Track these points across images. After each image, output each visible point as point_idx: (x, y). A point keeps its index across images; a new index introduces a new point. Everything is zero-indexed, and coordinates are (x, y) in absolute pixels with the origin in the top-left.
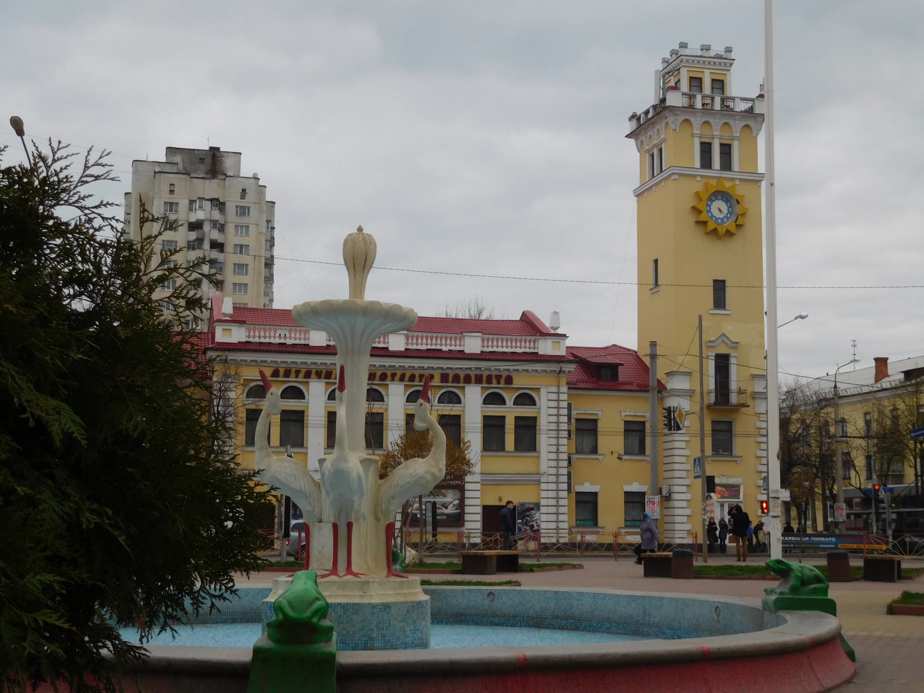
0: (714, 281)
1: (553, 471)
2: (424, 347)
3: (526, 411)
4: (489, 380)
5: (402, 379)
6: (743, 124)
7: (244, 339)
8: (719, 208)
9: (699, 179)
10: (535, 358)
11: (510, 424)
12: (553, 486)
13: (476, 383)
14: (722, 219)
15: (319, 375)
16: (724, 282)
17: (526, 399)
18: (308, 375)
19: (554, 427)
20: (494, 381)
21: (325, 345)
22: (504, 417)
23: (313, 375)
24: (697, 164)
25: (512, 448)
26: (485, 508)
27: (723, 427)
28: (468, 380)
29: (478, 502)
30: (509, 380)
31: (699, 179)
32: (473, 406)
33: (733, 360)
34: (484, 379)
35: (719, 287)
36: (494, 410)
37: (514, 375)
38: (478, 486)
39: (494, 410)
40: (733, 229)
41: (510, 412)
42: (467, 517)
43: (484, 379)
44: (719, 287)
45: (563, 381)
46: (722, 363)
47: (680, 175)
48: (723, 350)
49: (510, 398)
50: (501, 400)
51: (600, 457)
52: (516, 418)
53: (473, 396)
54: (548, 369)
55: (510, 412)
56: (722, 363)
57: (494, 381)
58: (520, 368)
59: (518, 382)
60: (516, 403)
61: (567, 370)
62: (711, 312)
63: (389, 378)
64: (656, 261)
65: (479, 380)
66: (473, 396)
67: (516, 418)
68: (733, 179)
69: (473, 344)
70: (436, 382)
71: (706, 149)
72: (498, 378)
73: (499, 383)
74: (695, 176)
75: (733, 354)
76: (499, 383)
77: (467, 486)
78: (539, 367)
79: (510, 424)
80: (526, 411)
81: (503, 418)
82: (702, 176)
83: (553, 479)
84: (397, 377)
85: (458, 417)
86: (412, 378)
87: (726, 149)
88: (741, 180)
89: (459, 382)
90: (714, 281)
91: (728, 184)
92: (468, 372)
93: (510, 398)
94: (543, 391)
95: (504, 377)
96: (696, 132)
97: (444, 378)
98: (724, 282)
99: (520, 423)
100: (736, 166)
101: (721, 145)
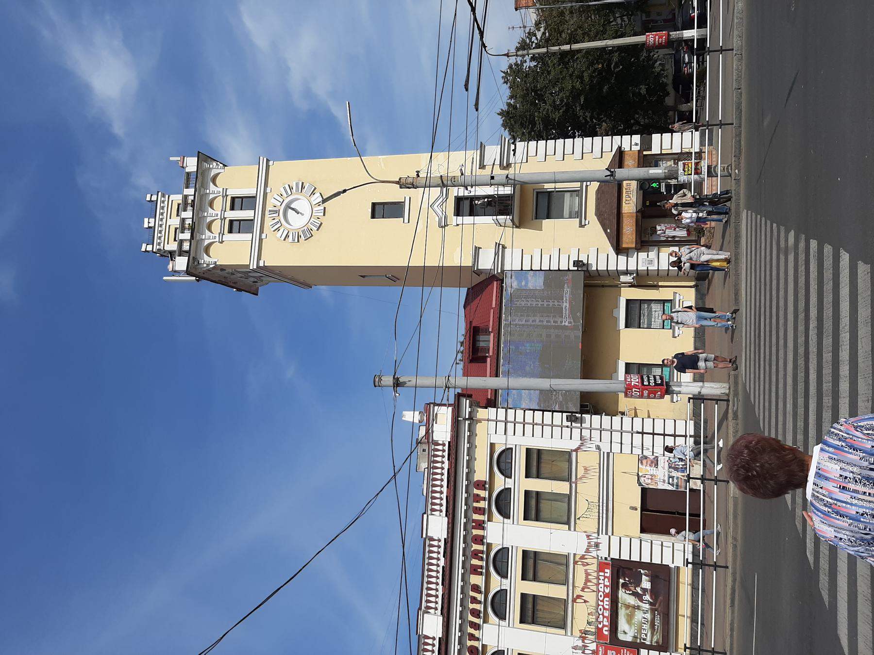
2: (440, 587)
3: (519, 463)
4: (480, 511)
13: (483, 528)
16: (374, 205)
17: (502, 461)
22: (527, 493)
24: (249, 236)
25: (566, 485)
26: (643, 531)
27: (544, 202)
28: (480, 540)
29: (636, 543)
30: (480, 485)
31: (264, 236)
32: (511, 534)
36: (518, 505)
38: (615, 541)
39: (518, 505)
41: (521, 484)
42: (657, 560)
45: (482, 413)
50: (505, 493)
52: (528, 476)
53: (500, 533)
54: (467, 434)
55: (521, 484)
56: (467, 206)
58: (465, 470)
59: (481, 474)
60: (507, 473)
61: (468, 410)
64: (363, 277)
65: (480, 525)
66: (500, 533)
67: (528, 476)
68: (265, 194)
71: (234, 226)
73: (484, 499)
74: (261, 240)
76: (484, 499)
77: (615, 555)
81: (527, 493)
82: (262, 232)
84: (476, 633)
85: (525, 553)
87: (236, 203)
90: (373, 217)
95: (476, 491)
96: (217, 239)
97: (475, 570)
98: (374, 205)
100: (251, 192)
101: (232, 208)
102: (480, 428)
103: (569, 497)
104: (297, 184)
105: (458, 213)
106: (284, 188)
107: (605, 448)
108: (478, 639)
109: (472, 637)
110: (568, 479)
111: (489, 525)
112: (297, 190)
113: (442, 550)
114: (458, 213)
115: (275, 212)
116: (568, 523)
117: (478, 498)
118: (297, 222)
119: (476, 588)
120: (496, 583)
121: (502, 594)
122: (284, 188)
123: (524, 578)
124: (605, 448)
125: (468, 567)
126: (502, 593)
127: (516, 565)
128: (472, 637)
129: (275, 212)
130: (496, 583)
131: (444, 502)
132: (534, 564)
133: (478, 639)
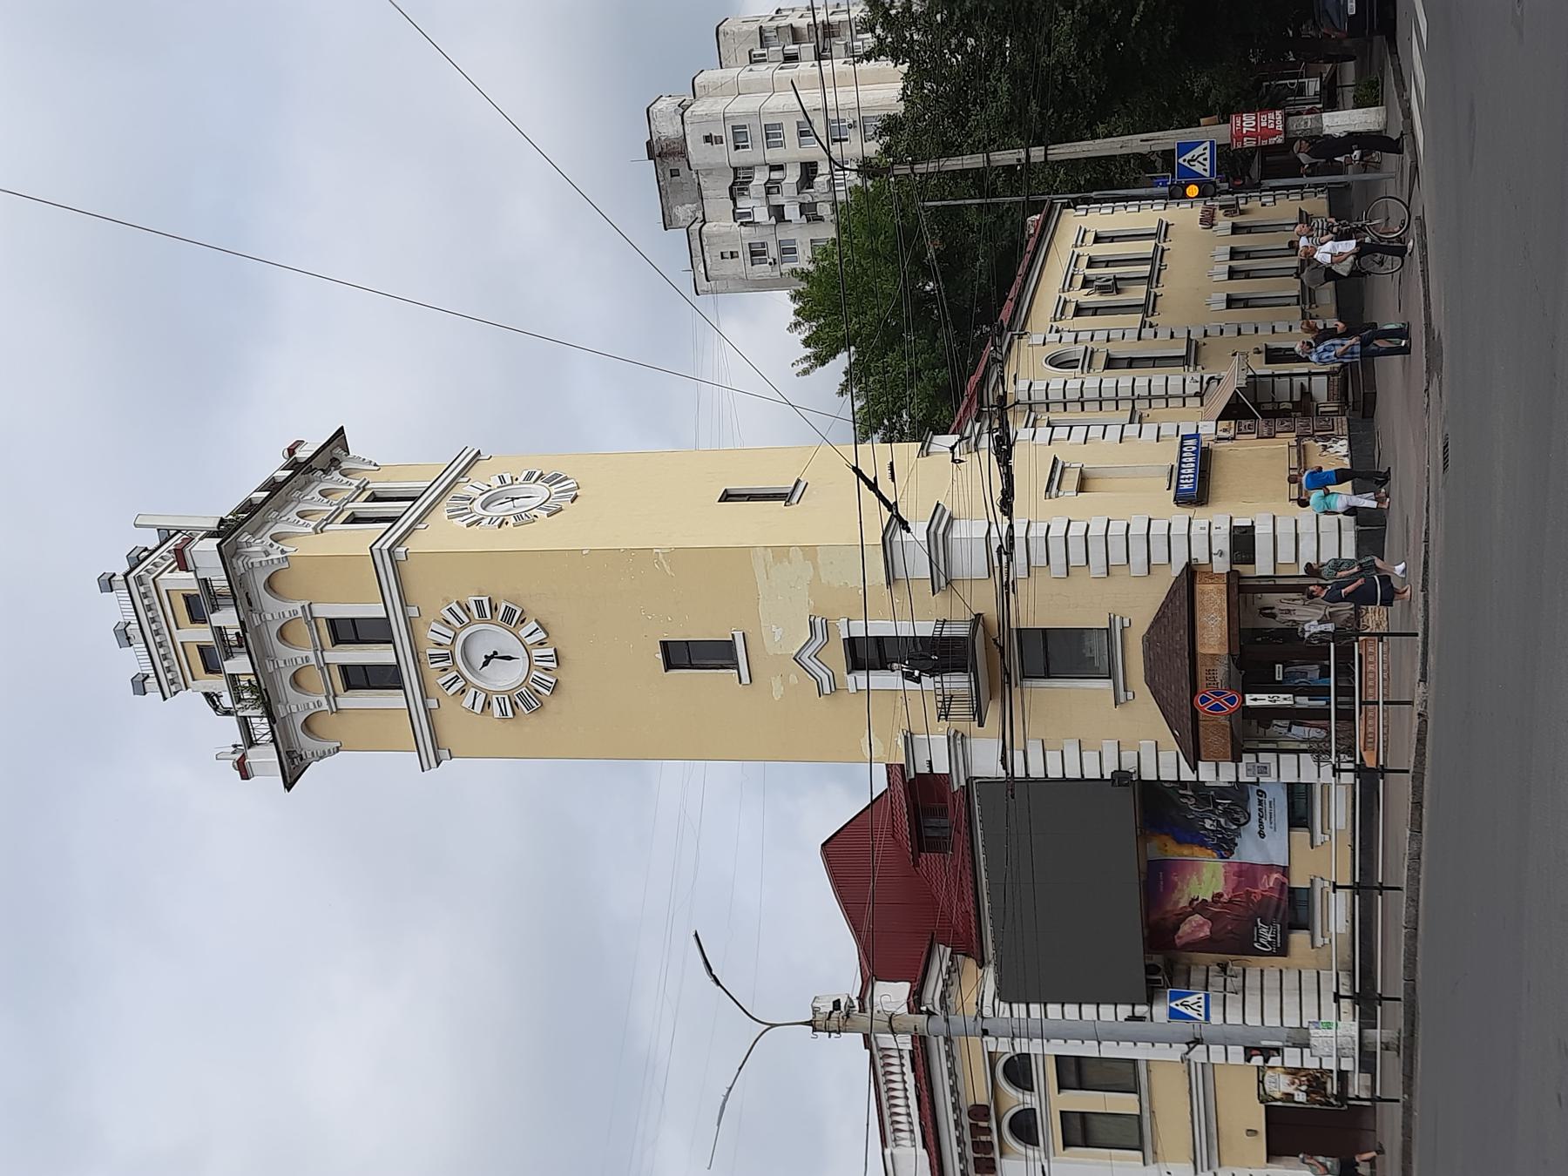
0: (669, 666)
3: (1045, 1075)
6: (266, 597)
9: (432, 704)
35: (677, 655)
37: (967, 1101)
39: (1051, 1130)
44: (677, 655)
48: (837, 656)
49: (1015, 1099)
52: (1062, 1087)
62: (746, 680)
67: (1062, 1087)
68: (408, 621)
80: (1045, 1075)
88: (404, 603)
93: (1015, 1099)
99: (1072, 1079)
103: (1139, 1117)
104: (479, 604)
106: (450, 610)
110: (1135, 1089)
112: (482, 614)
115: (446, 657)
116: (1140, 1148)
118: (507, 677)
122: (450, 610)
129: (446, 657)
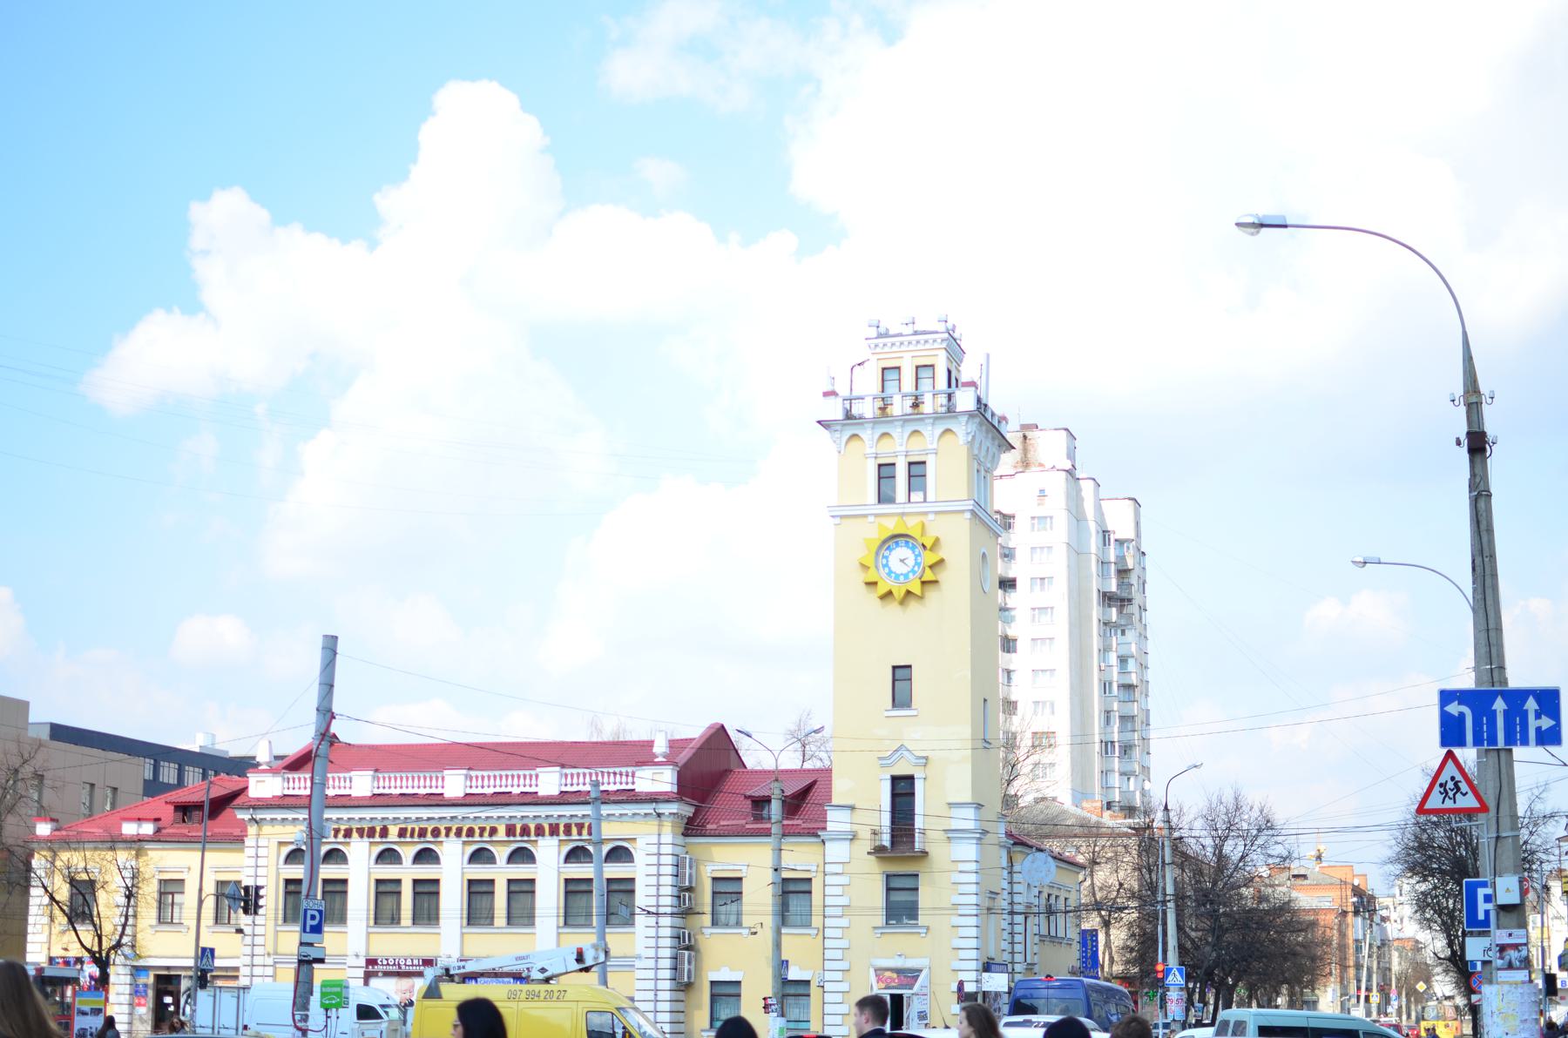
1: (652, 953)
2: (491, 790)
4: (568, 831)
5: (459, 833)
6: (939, 429)
7: (279, 793)
8: (902, 560)
10: (631, 797)
11: (598, 889)
12: (651, 974)
14: (906, 576)
15: (361, 832)
17: (620, 854)
18: (348, 834)
19: (653, 891)
20: (574, 830)
21: (369, 794)
23: (355, 835)
28: (540, 831)
31: (871, 519)
32: (549, 866)
33: (919, 786)
34: (562, 829)
35: (901, 674)
40: (916, 588)
43: (562, 829)
44: (901, 674)
46: (902, 789)
47: (842, 517)
51: (745, 932)
54: (642, 812)
56: (902, 789)
57: (574, 830)
63: (443, 832)
65: (554, 831)
68: (926, 513)
69: (549, 781)
70: (501, 834)
71: (885, 472)
72: (580, 827)
73: (580, 833)
74: (865, 516)
75: (918, 774)
76: (580, 833)
78: (629, 809)
79: (598, 889)
82: (876, 515)
83: (651, 963)
86: (471, 832)
87: (917, 470)
88: (936, 513)
89: (529, 835)
91: (911, 526)
92: (538, 821)
94: (640, 843)
97: (510, 831)
102: (652, 826)
105: (895, 779)
107: (638, 964)
108: (447, 835)
109: (448, 830)
111: (554, 841)
113: (527, 789)
114: (895, 779)
117: (580, 827)
119: (493, 831)
120: (501, 853)
121: (491, 859)
123: (509, 881)
124: (638, 964)
125: (513, 822)
126: (491, 859)
127: (521, 871)
128: (448, 830)
130: (501, 853)
131: (575, 788)
132: (522, 890)
133: (447, 835)
